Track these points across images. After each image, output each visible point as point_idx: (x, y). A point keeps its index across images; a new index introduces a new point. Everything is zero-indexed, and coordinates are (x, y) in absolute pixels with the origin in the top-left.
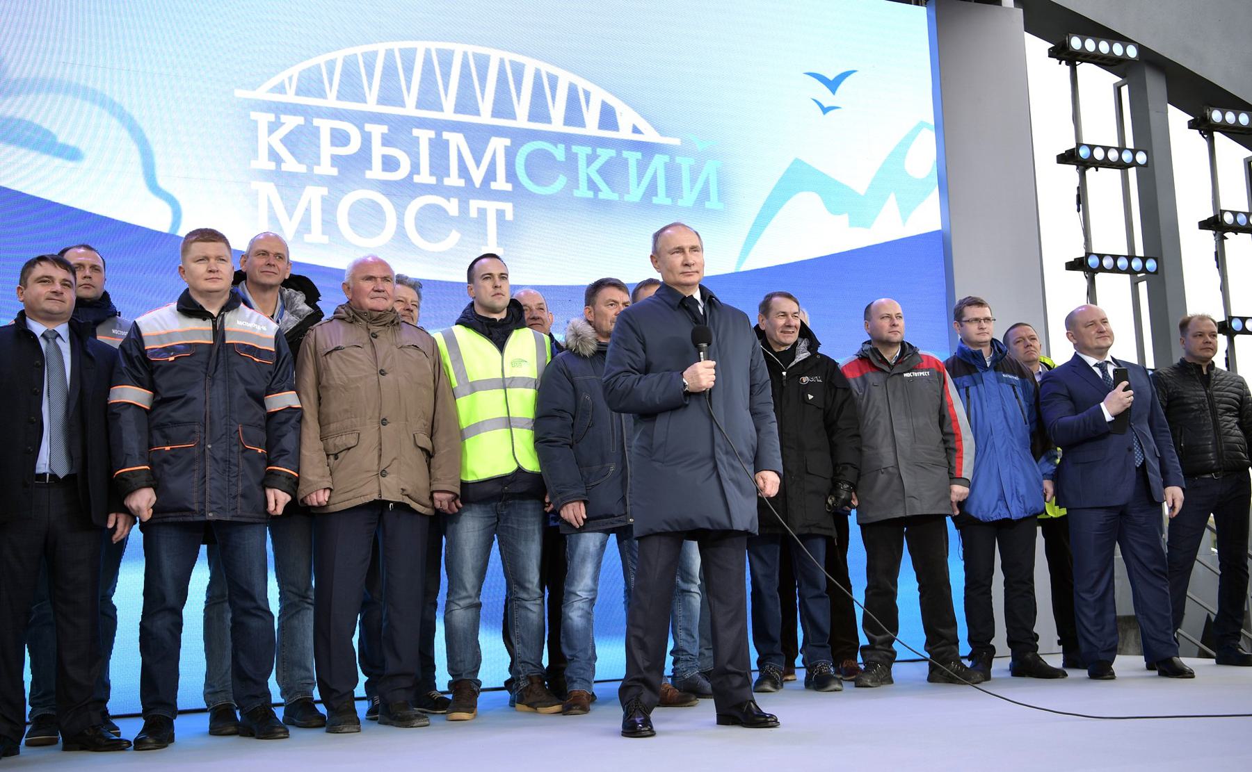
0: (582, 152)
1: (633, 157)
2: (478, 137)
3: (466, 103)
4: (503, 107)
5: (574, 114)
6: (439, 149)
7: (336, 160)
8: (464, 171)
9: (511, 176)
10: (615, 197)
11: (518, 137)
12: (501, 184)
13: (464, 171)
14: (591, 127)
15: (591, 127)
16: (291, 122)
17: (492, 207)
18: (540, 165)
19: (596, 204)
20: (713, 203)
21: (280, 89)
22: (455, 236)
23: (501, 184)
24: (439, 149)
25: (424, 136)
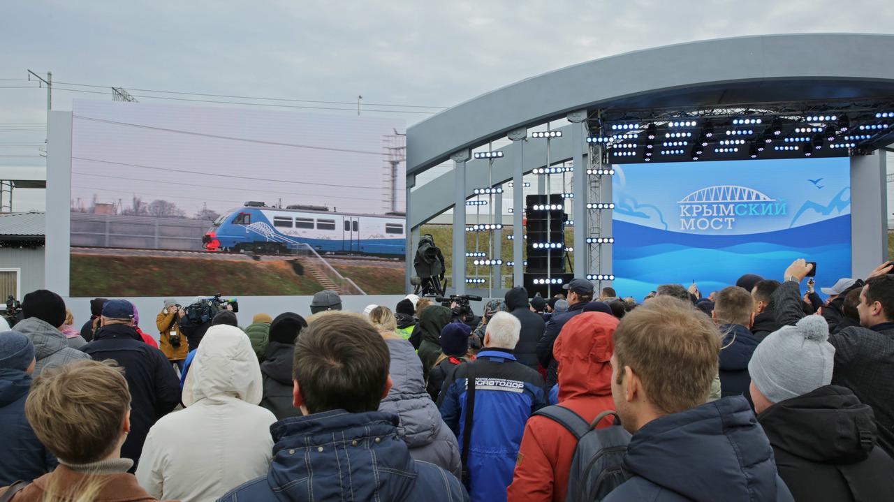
0: (751, 205)
1: (763, 205)
2: (727, 205)
3: (724, 198)
4: (733, 198)
5: (749, 197)
6: (718, 208)
7: (696, 213)
8: (723, 212)
9: (734, 212)
10: (758, 214)
11: (736, 204)
12: (732, 214)
13: (723, 212)
14: (753, 199)
15: (753, 199)
16: (688, 206)
17: (730, 219)
18: (741, 210)
19: (754, 217)
20: (784, 213)
21: (685, 200)
22: (721, 226)
23: (732, 214)
24: (718, 208)
25: (715, 206)
